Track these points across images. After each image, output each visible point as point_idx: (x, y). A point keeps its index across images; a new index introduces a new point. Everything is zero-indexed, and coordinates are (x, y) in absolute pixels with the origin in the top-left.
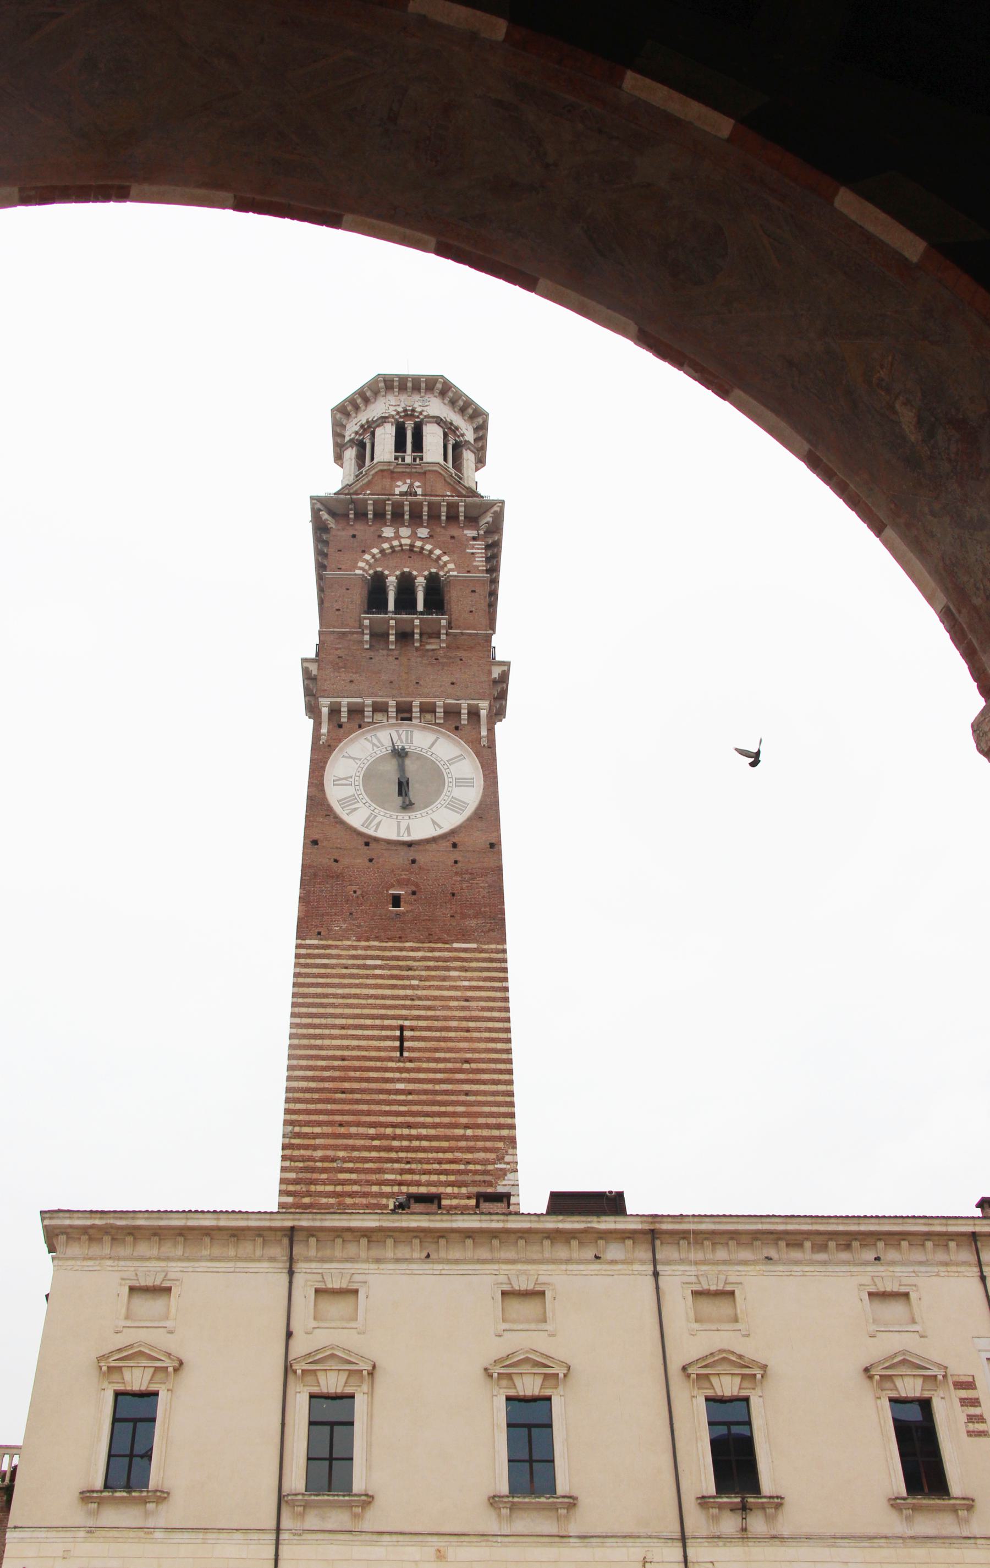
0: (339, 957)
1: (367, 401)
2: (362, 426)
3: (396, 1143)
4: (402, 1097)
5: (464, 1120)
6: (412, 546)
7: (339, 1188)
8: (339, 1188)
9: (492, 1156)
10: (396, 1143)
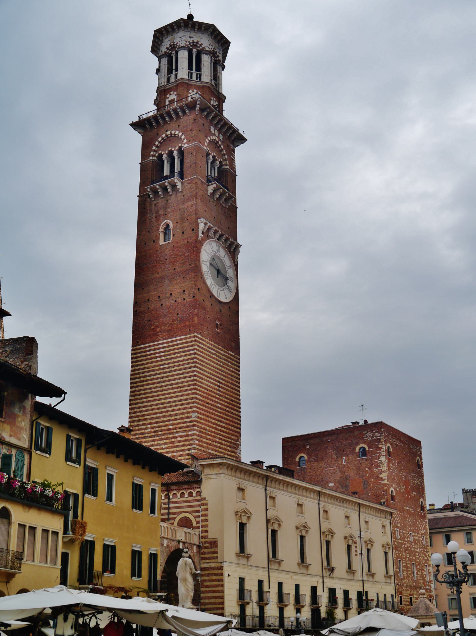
0: (205, 345)
2: (193, 42)
3: (218, 427)
4: (219, 410)
5: (231, 423)
6: (218, 142)
7: (207, 441)
8: (207, 441)
9: (236, 438)
10: (218, 427)
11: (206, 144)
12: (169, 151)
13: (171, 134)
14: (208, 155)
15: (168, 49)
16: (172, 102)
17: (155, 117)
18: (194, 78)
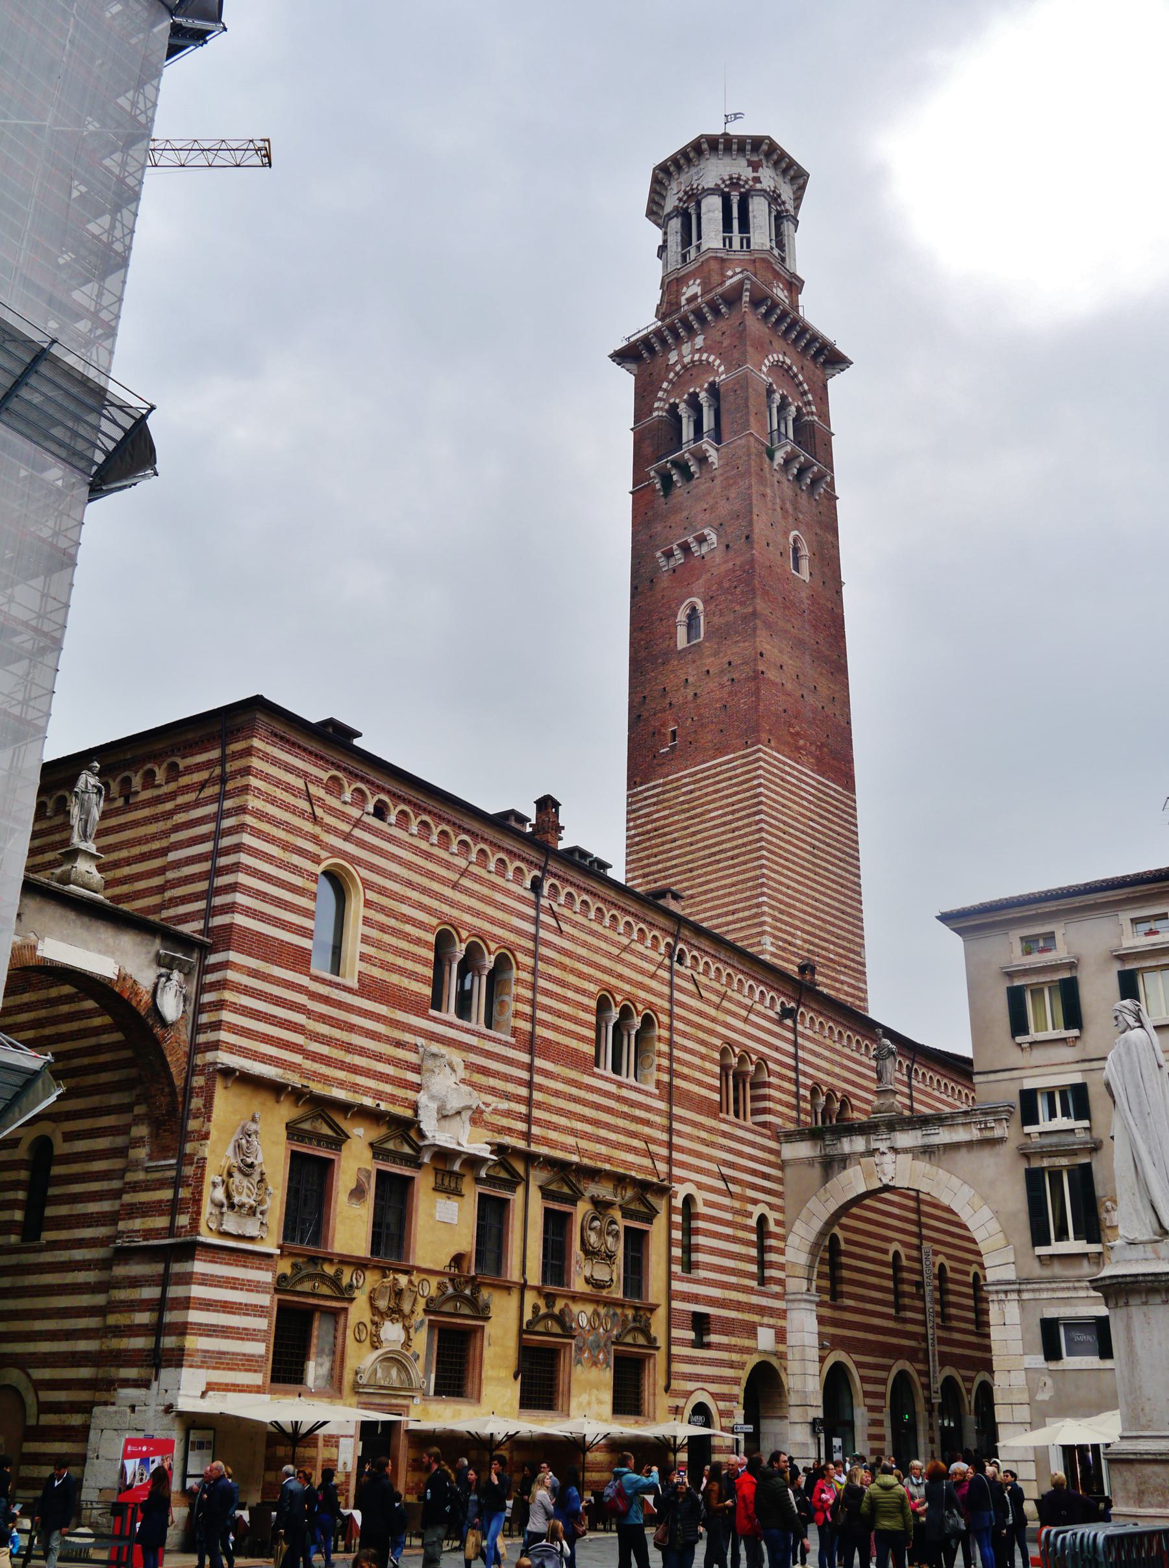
11: (764, 369)
12: (690, 395)
13: (693, 361)
14: (770, 392)
15: (680, 200)
16: (694, 298)
17: (658, 333)
18: (736, 245)
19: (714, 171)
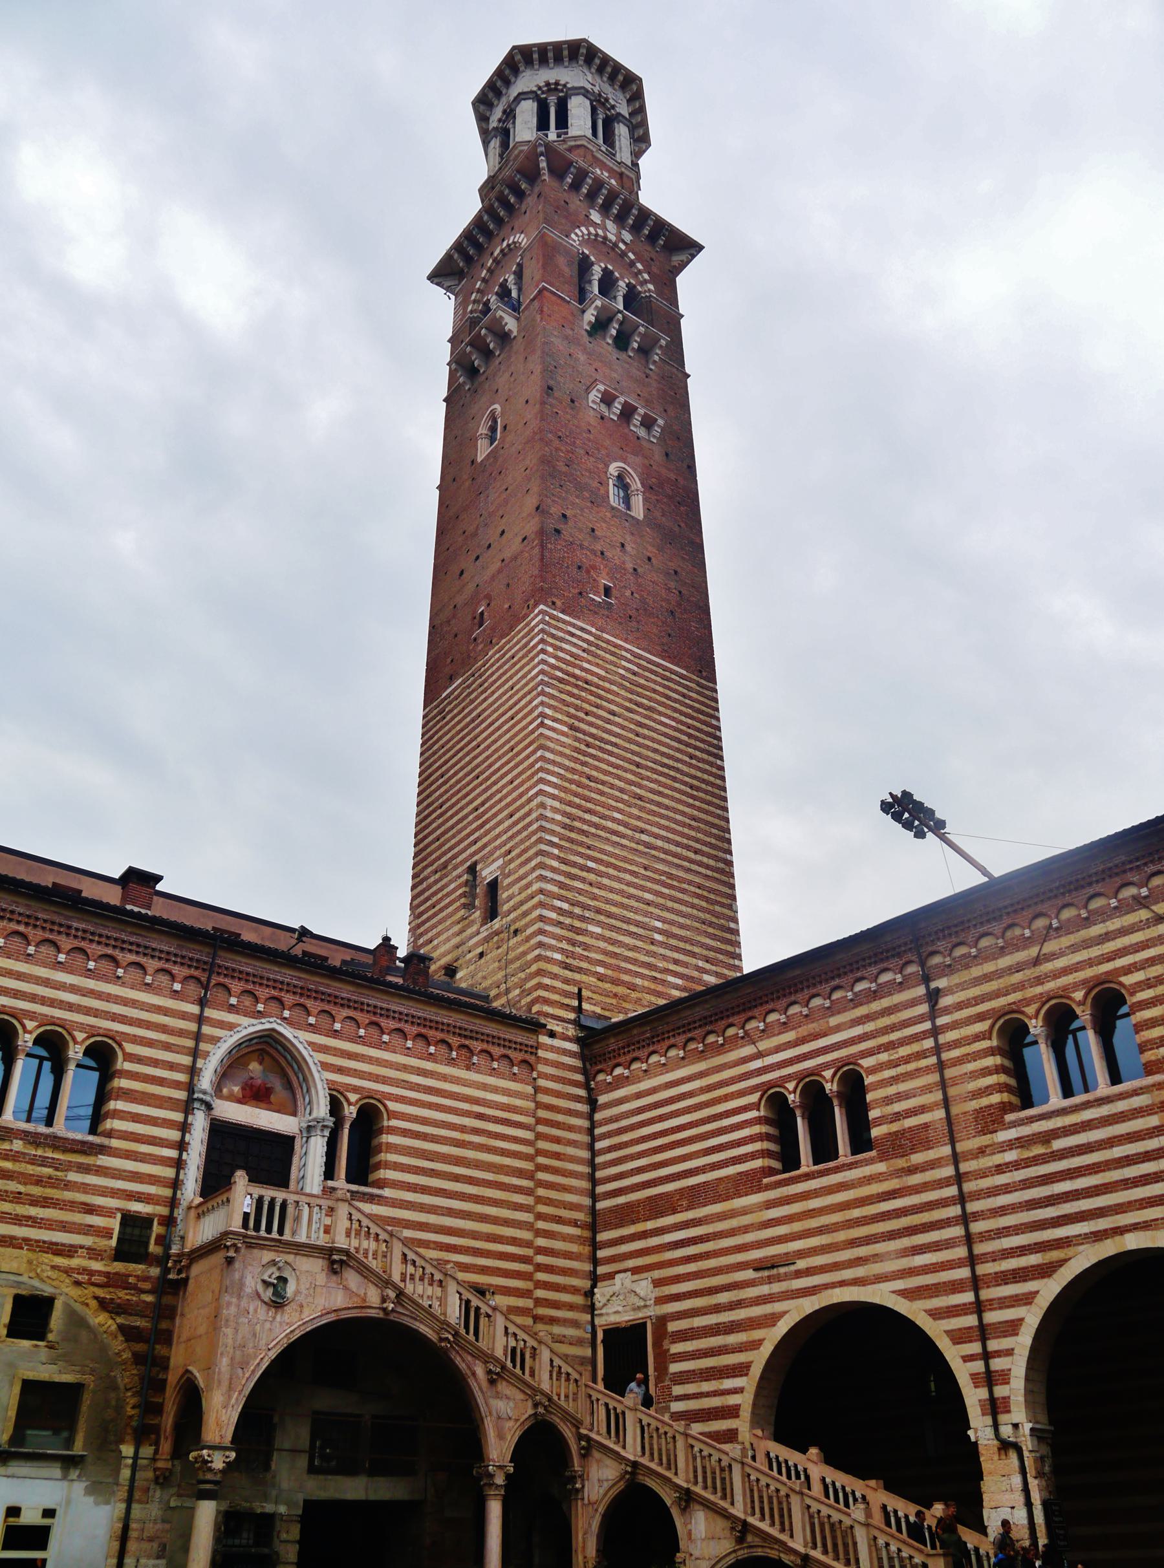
1: (558, 60)
2: (548, 84)
6: (616, 245)
15: (500, 120)
19: (530, 80)
